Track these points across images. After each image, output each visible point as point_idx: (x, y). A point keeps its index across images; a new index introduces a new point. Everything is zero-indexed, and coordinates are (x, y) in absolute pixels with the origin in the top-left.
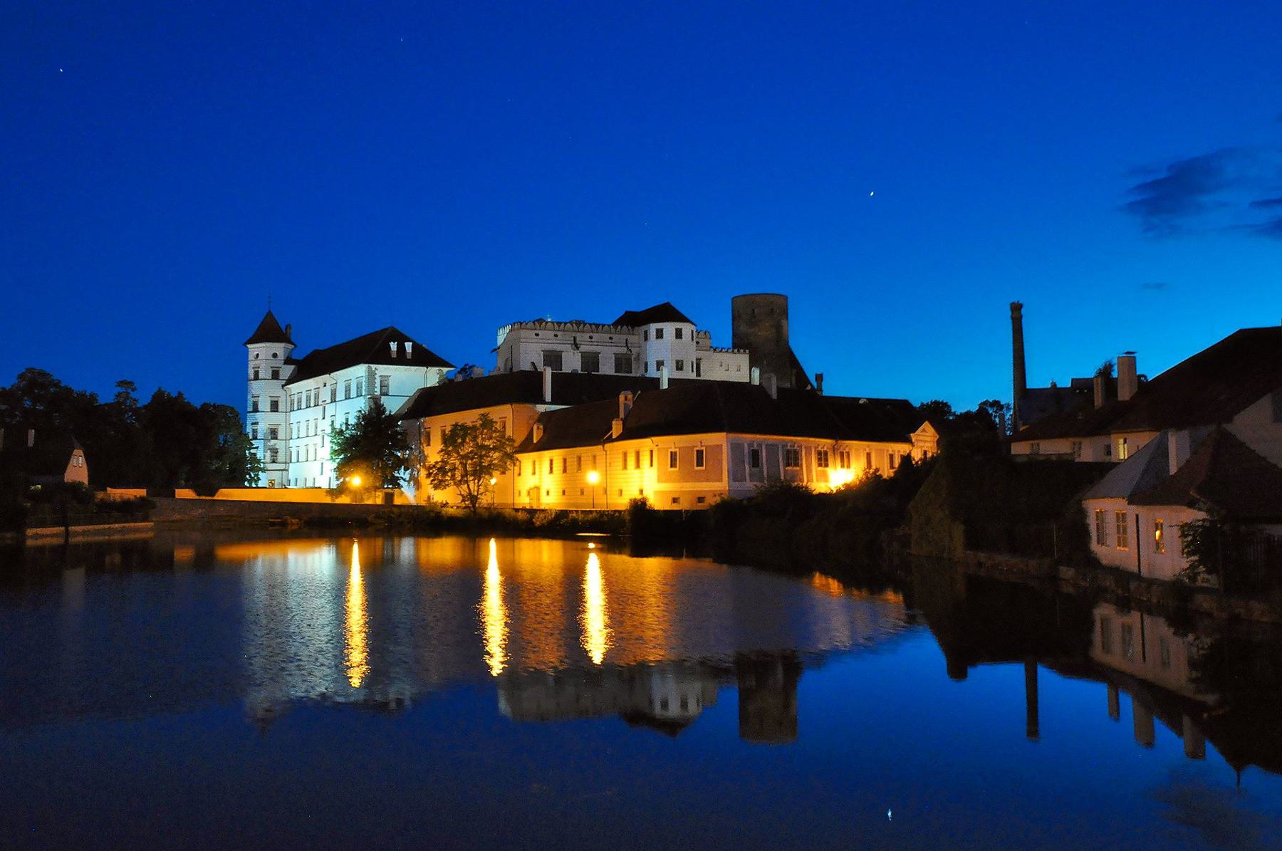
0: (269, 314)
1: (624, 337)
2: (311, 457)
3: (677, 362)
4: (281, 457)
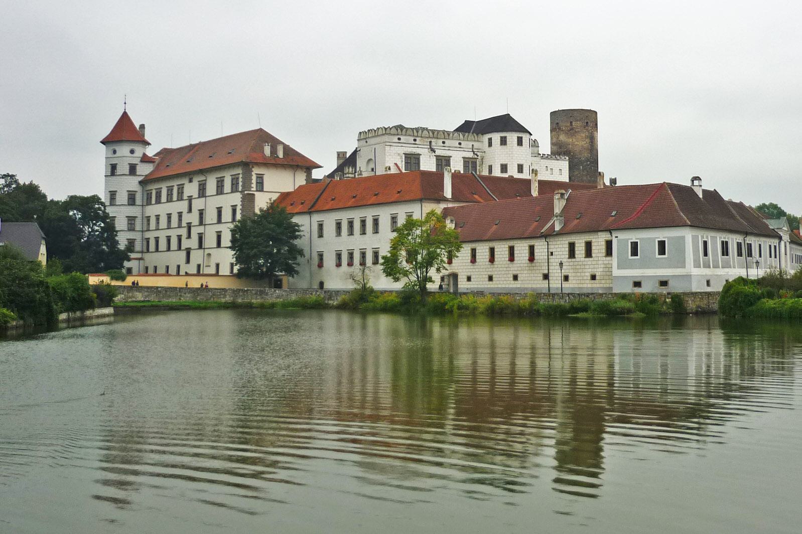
0: (125, 116)
1: (470, 144)
2: (174, 245)
3: (519, 165)
4: (138, 246)
